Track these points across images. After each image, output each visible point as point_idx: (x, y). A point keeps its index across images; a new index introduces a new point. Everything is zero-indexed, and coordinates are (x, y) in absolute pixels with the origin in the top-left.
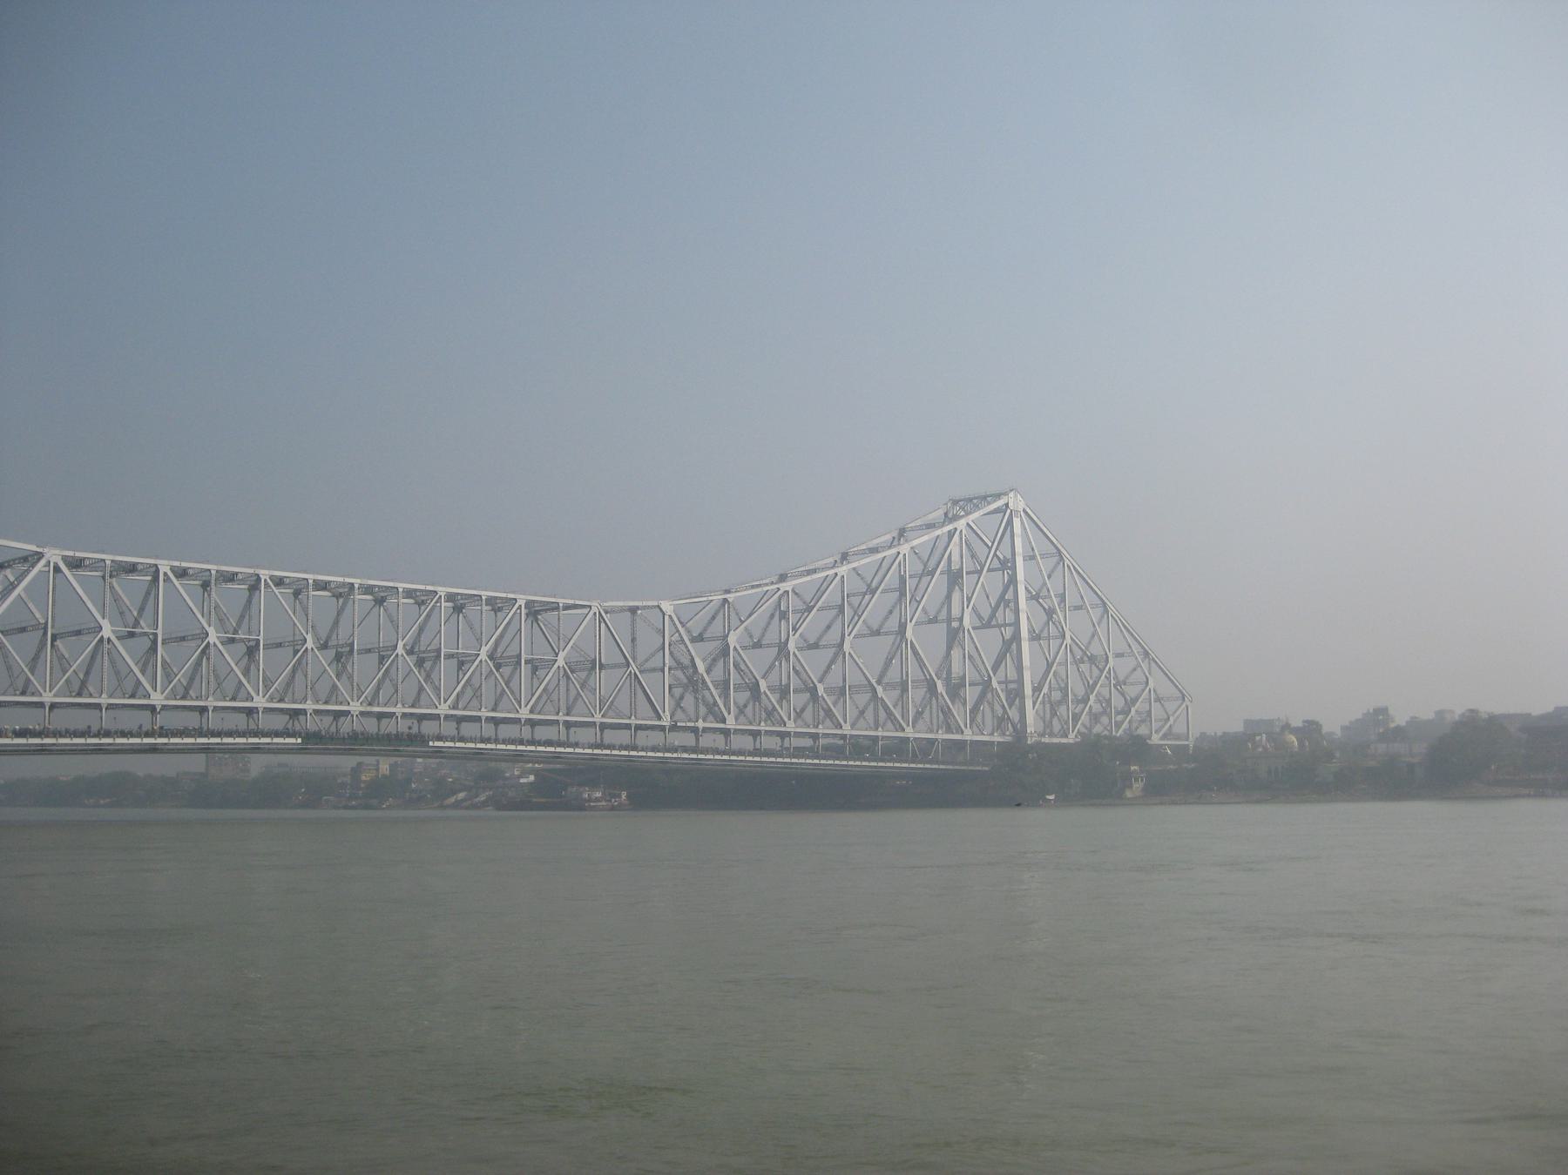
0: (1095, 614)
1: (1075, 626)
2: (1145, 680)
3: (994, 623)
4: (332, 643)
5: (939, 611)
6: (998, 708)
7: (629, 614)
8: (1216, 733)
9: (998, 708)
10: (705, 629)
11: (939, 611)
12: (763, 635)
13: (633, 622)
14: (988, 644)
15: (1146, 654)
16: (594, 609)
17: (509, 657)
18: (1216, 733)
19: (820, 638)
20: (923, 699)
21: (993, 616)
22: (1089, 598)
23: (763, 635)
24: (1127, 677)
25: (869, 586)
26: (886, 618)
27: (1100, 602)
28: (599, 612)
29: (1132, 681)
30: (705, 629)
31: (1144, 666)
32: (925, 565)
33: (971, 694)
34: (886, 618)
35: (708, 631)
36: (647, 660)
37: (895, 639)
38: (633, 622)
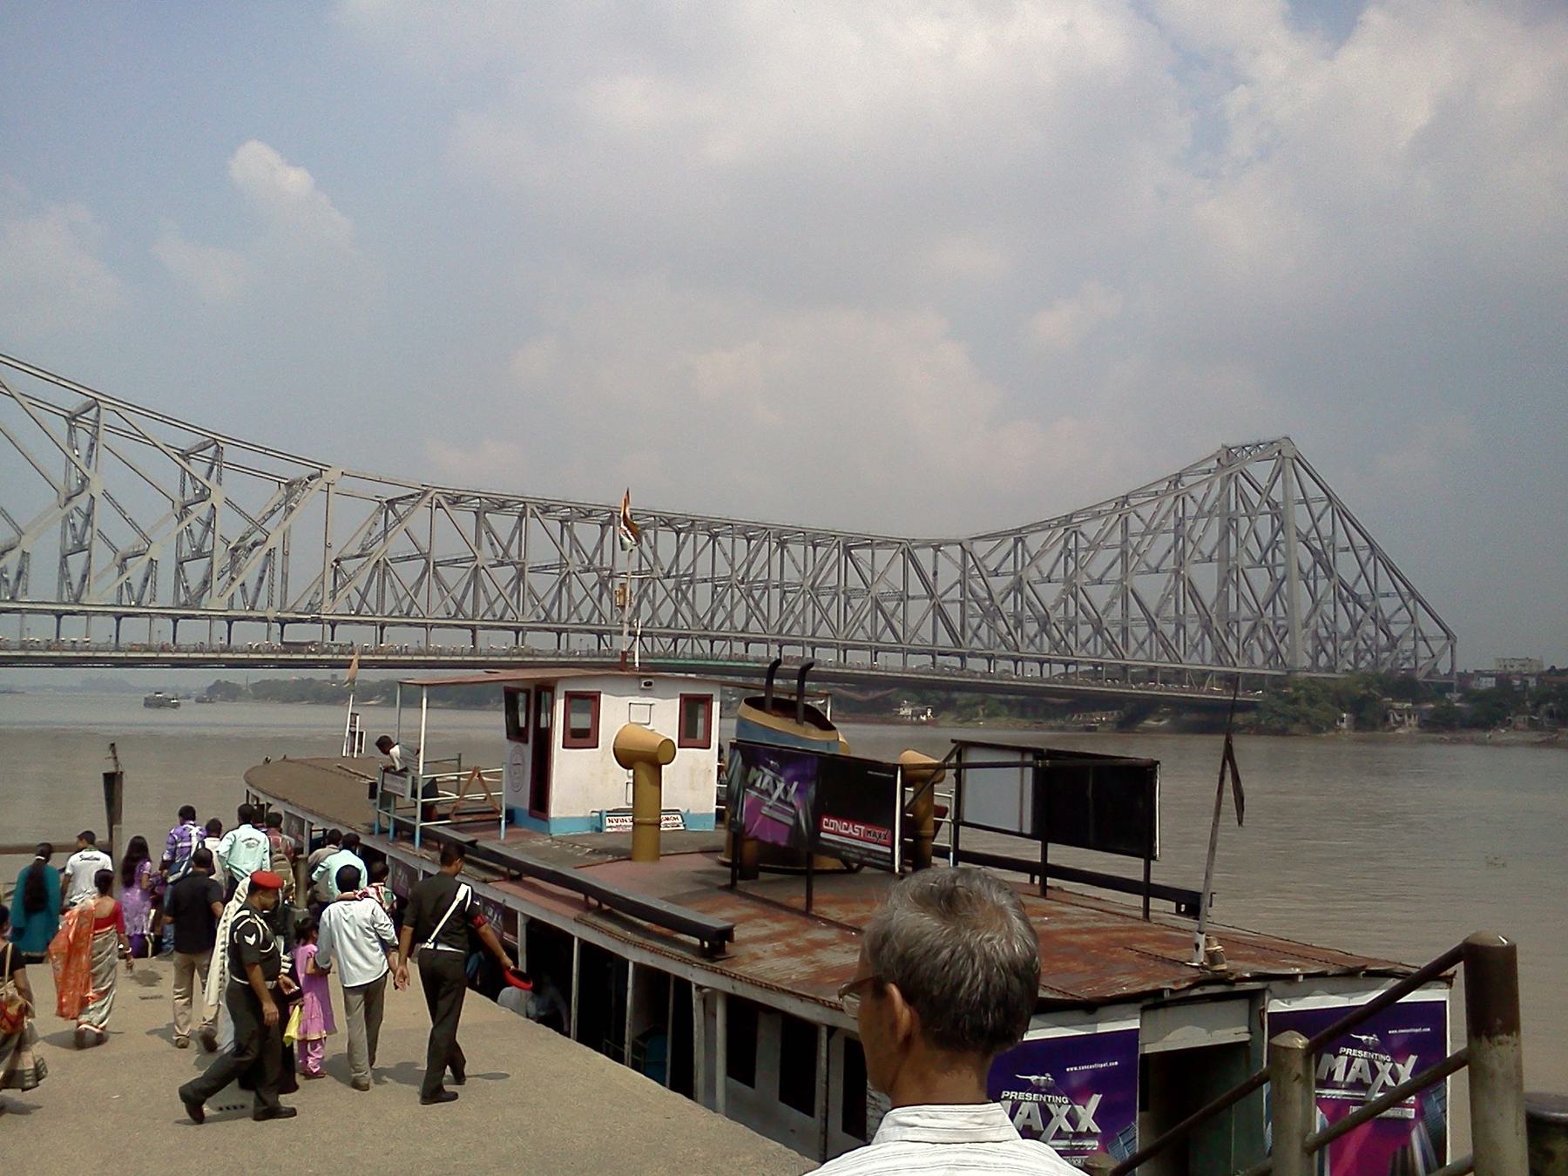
0: (1364, 555)
1: (1347, 567)
2: (1410, 619)
3: (1263, 563)
4: (674, 573)
5: (1213, 551)
6: (1270, 646)
7: (932, 549)
8: (1465, 671)
9: (1270, 646)
10: (1000, 565)
11: (1213, 551)
12: (1052, 571)
13: (936, 556)
14: (1261, 580)
15: (1413, 594)
16: (903, 546)
17: (761, 582)
18: (1465, 671)
19: (1103, 575)
20: (1196, 633)
21: (1264, 558)
22: (1359, 540)
23: (1052, 571)
24: (1392, 616)
25: (1148, 527)
26: (1165, 556)
27: (1367, 544)
28: (908, 549)
29: (1396, 620)
30: (1000, 565)
31: (1411, 604)
32: (1200, 509)
33: (1246, 627)
34: (1165, 556)
35: (1003, 567)
36: (946, 592)
37: (1171, 576)
38: (936, 556)
